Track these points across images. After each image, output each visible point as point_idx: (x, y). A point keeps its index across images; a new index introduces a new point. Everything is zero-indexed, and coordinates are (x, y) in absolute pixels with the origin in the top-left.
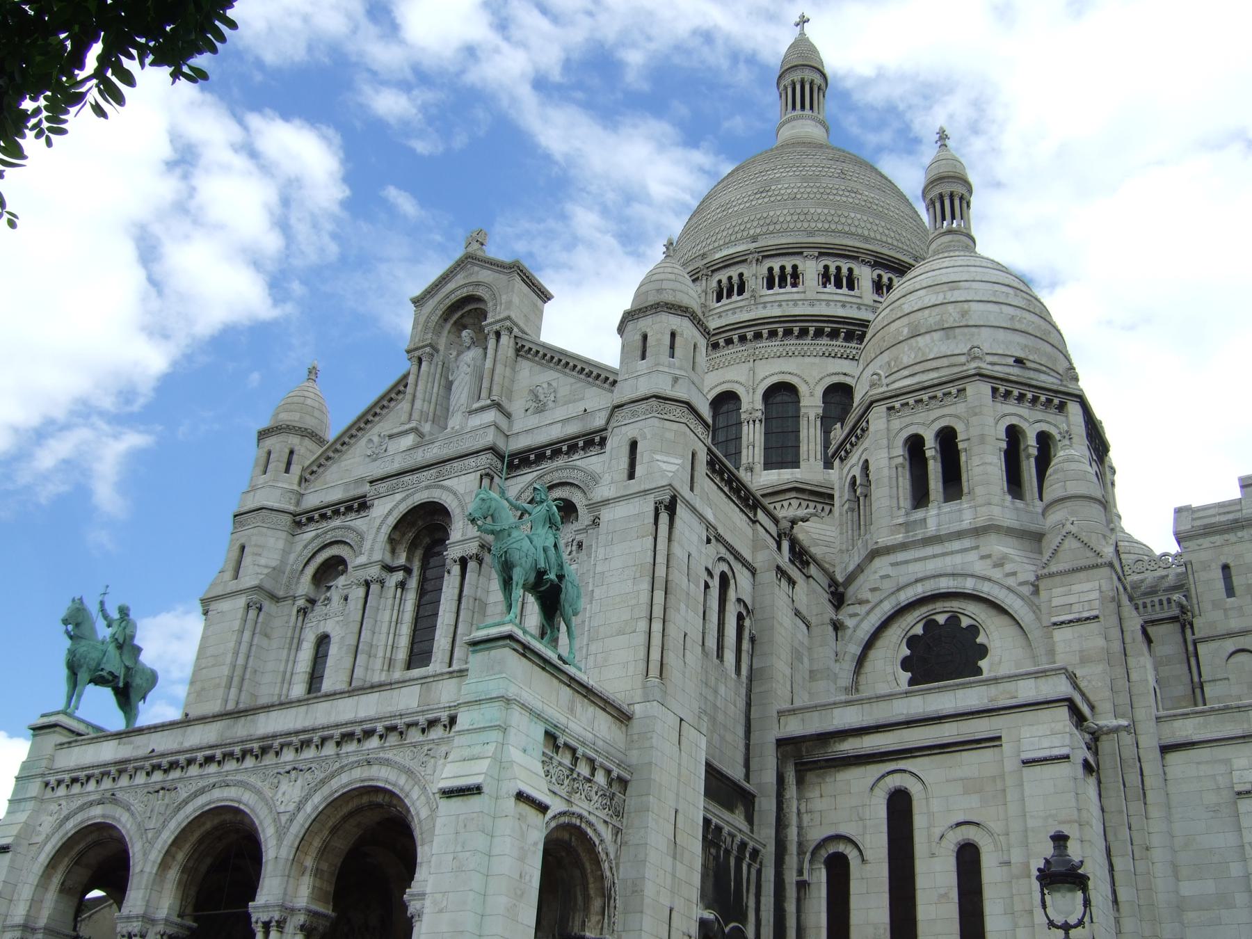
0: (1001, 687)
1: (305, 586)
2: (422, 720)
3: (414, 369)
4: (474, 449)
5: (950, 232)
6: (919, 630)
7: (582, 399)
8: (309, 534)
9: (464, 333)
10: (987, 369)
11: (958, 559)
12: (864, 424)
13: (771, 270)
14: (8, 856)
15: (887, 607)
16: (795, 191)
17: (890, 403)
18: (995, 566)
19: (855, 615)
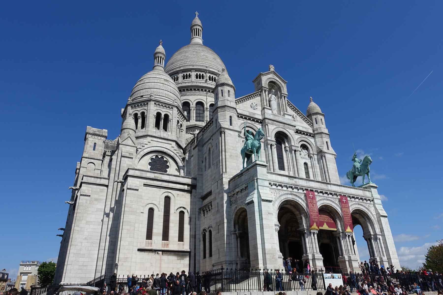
3: (264, 92)
7: (303, 123)
8: (242, 121)
14: (271, 204)
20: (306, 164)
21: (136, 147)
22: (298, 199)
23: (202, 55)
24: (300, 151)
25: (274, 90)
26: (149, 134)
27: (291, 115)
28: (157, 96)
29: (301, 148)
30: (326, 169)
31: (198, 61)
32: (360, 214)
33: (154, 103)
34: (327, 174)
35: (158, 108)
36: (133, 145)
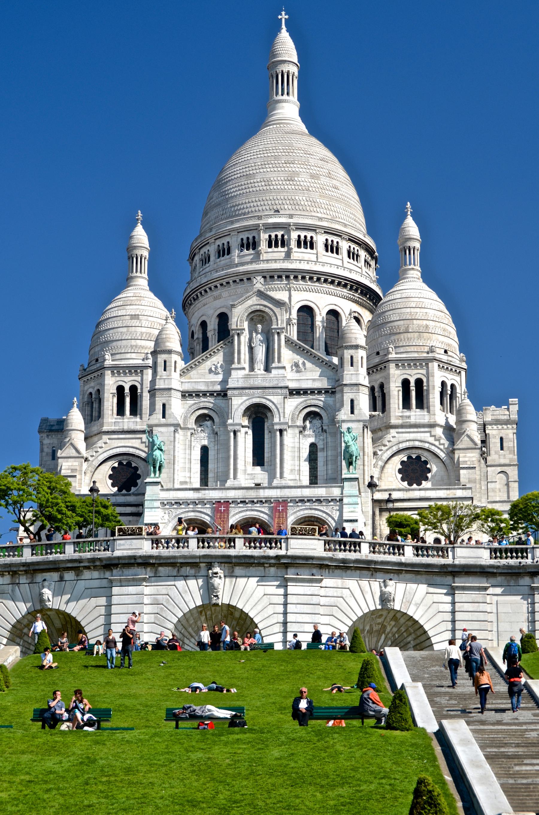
0: (451, 491)
1: (191, 423)
2: (330, 499)
3: (236, 338)
4: (280, 385)
5: (413, 269)
6: (405, 459)
8: (190, 402)
9: (260, 326)
10: (438, 356)
11: (422, 434)
12: (383, 367)
13: (299, 236)
15: (395, 449)
16: (309, 184)
17: (397, 362)
18: (436, 440)
19: (381, 450)
20: (313, 446)
21: (83, 457)
22: (203, 516)
23: (258, 180)
24: (298, 427)
25: (260, 326)
26: (105, 428)
27: (284, 368)
28: (118, 357)
29: (309, 418)
30: (339, 451)
31: (247, 201)
32: (316, 522)
33: (109, 372)
34: (339, 457)
35: (118, 379)
36: (77, 455)
